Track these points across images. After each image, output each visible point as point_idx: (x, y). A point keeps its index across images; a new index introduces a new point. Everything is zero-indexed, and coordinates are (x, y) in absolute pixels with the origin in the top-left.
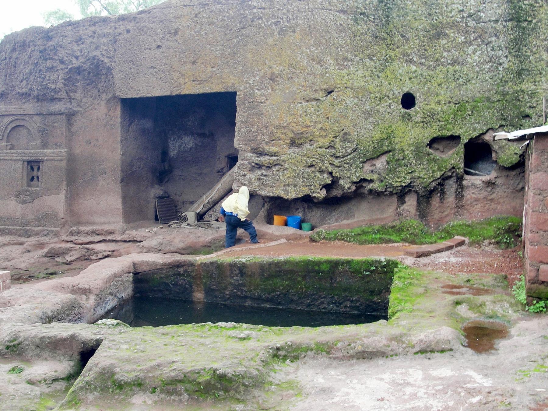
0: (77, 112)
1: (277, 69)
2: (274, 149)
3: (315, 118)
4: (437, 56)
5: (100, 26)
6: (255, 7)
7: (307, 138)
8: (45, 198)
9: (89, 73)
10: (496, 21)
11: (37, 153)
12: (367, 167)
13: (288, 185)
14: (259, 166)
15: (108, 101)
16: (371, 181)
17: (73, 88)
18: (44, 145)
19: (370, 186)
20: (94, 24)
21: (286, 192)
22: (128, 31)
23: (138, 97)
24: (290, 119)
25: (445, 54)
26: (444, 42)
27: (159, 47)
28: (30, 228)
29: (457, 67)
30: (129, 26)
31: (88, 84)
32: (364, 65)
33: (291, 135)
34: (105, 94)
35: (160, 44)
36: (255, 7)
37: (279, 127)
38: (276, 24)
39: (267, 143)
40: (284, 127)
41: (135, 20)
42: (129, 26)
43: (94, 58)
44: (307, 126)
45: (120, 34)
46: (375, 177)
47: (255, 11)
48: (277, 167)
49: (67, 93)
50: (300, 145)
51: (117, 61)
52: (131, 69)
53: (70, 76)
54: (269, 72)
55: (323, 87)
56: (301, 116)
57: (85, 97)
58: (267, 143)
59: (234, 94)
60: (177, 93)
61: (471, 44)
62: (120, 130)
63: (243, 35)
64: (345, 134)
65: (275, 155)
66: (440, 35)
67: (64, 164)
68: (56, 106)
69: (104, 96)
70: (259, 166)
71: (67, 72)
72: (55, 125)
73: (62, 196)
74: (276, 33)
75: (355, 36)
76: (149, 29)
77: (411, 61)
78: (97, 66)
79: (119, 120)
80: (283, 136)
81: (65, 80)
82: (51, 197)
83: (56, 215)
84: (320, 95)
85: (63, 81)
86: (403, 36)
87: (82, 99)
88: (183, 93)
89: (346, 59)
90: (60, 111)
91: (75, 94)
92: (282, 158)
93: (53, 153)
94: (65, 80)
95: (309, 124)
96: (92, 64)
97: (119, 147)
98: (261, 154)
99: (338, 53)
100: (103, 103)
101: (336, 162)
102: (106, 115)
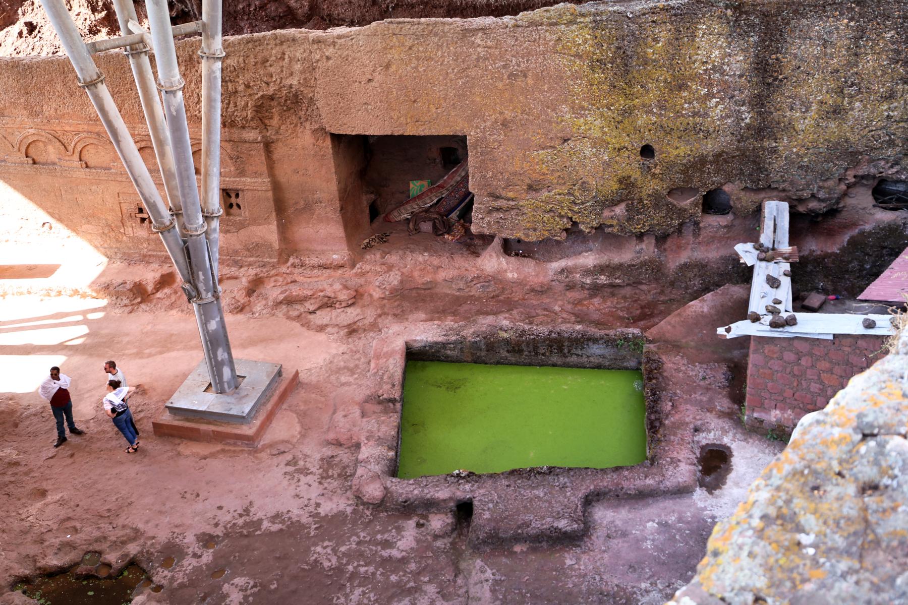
0: (278, 140)
1: (508, 114)
2: (511, 195)
3: (552, 167)
4: (678, 108)
5: (289, 47)
6: (479, 46)
7: (545, 185)
8: (253, 228)
9: (286, 101)
10: (741, 76)
11: (234, 182)
12: (607, 213)
13: (529, 229)
14: (498, 210)
15: (314, 132)
16: (611, 226)
17: (267, 114)
18: (240, 173)
19: (610, 230)
20: (282, 43)
21: (527, 235)
22: (328, 58)
23: (354, 133)
24: (526, 166)
25: (686, 106)
26: (685, 94)
27: (370, 80)
28: (239, 258)
29: (698, 119)
30: (330, 51)
31: (285, 111)
32: (602, 115)
33: (528, 181)
34: (308, 123)
35: (370, 77)
36: (479, 46)
37: (515, 174)
38: (504, 67)
39: (503, 189)
40: (521, 174)
41: (334, 46)
42: (330, 51)
43: (291, 86)
44: (544, 174)
45: (318, 61)
46: (615, 222)
47: (479, 49)
48: (515, 211)
49: (261, 120)
50: (536, 190)
51: (321, 93)
52: (340, 103)
53: (262, 103)
54: (501, 118)
55: (559, 135)
56: (537, 164)
57: (282, 124)
58: (503, 189)
59: (463, 139)
60: (400, 133)
61: (713, 97)
62: (332, 161)
63: (467, 76)
64: (584, 183)
65: (513, 200)
66: (681, 87)
67: (270, 194)
68: (251, 134)
69: (307, 125)
70: (498, 210)
71: (258, 99)
72: (252, 153)
73: (274, 227)
74: (506, 77)
75: (592, 85)
76: (355, 59)
77: (650, 112)
78: (296, 96)
79: (331, 151)
80: (519, 182)
81: (256, 107)
82: (261, 227)
83: (271, 246)
84: (557, 143)
85: (254, 109)
86: (642, 87)
87: (280, 127)
88: (406, 134)
89: (582, 108)
90: (256, 139)
91: (271, 121)
92: (521, 203)
93: (255, 182)
94: (256, 107)
95: (547, 172)
96: (289, 93)
97: (334, 177)
98: (498, 197)
99: (573, 102)
100: (308, 132)
101: (576, 208)
102: (314, 145)
